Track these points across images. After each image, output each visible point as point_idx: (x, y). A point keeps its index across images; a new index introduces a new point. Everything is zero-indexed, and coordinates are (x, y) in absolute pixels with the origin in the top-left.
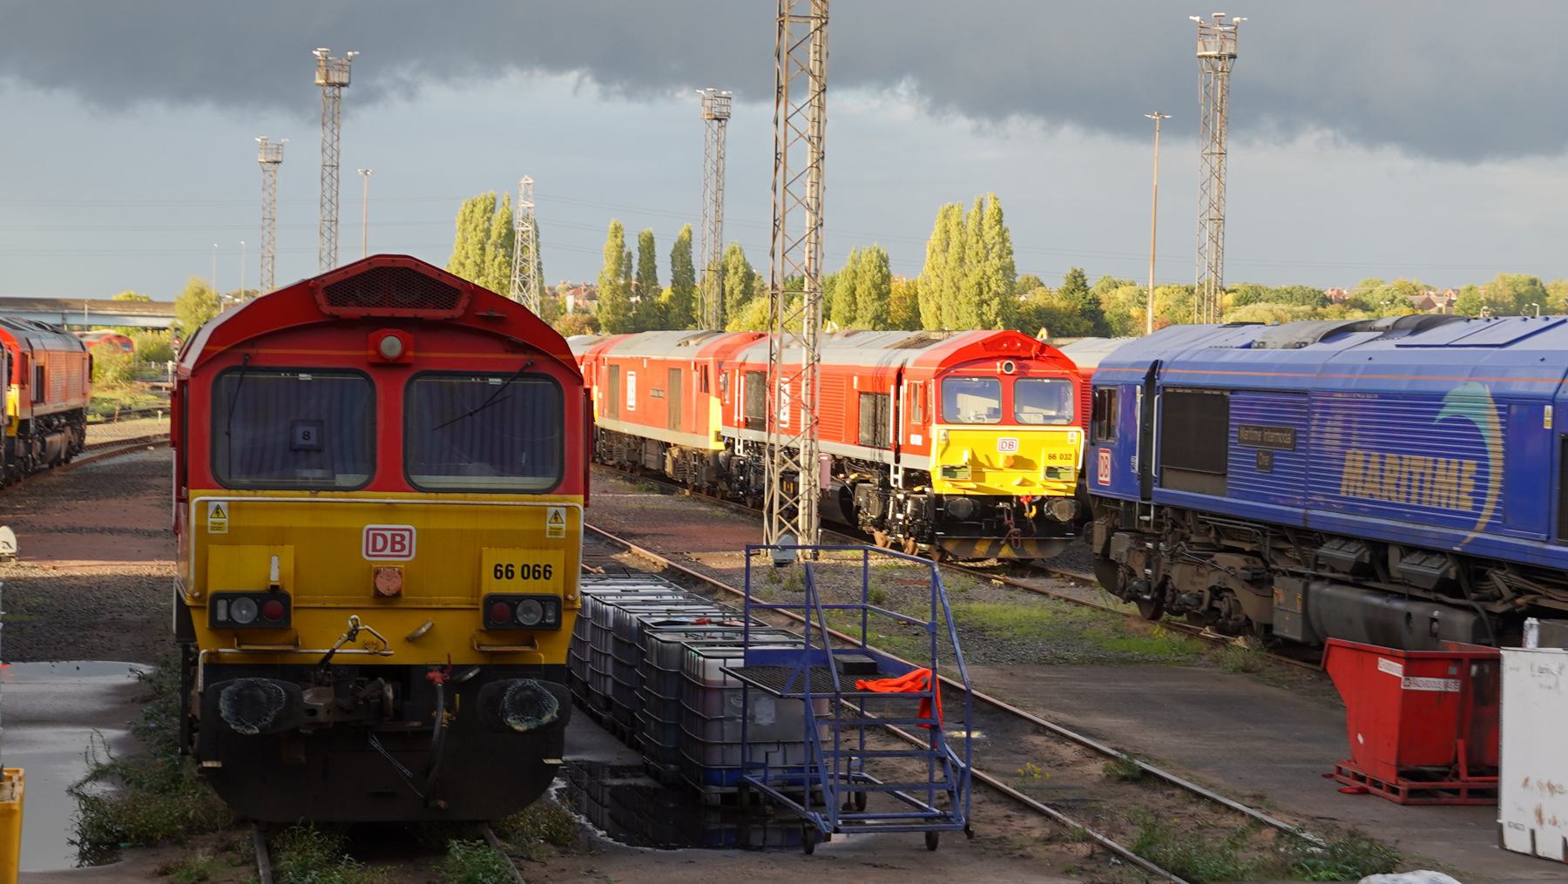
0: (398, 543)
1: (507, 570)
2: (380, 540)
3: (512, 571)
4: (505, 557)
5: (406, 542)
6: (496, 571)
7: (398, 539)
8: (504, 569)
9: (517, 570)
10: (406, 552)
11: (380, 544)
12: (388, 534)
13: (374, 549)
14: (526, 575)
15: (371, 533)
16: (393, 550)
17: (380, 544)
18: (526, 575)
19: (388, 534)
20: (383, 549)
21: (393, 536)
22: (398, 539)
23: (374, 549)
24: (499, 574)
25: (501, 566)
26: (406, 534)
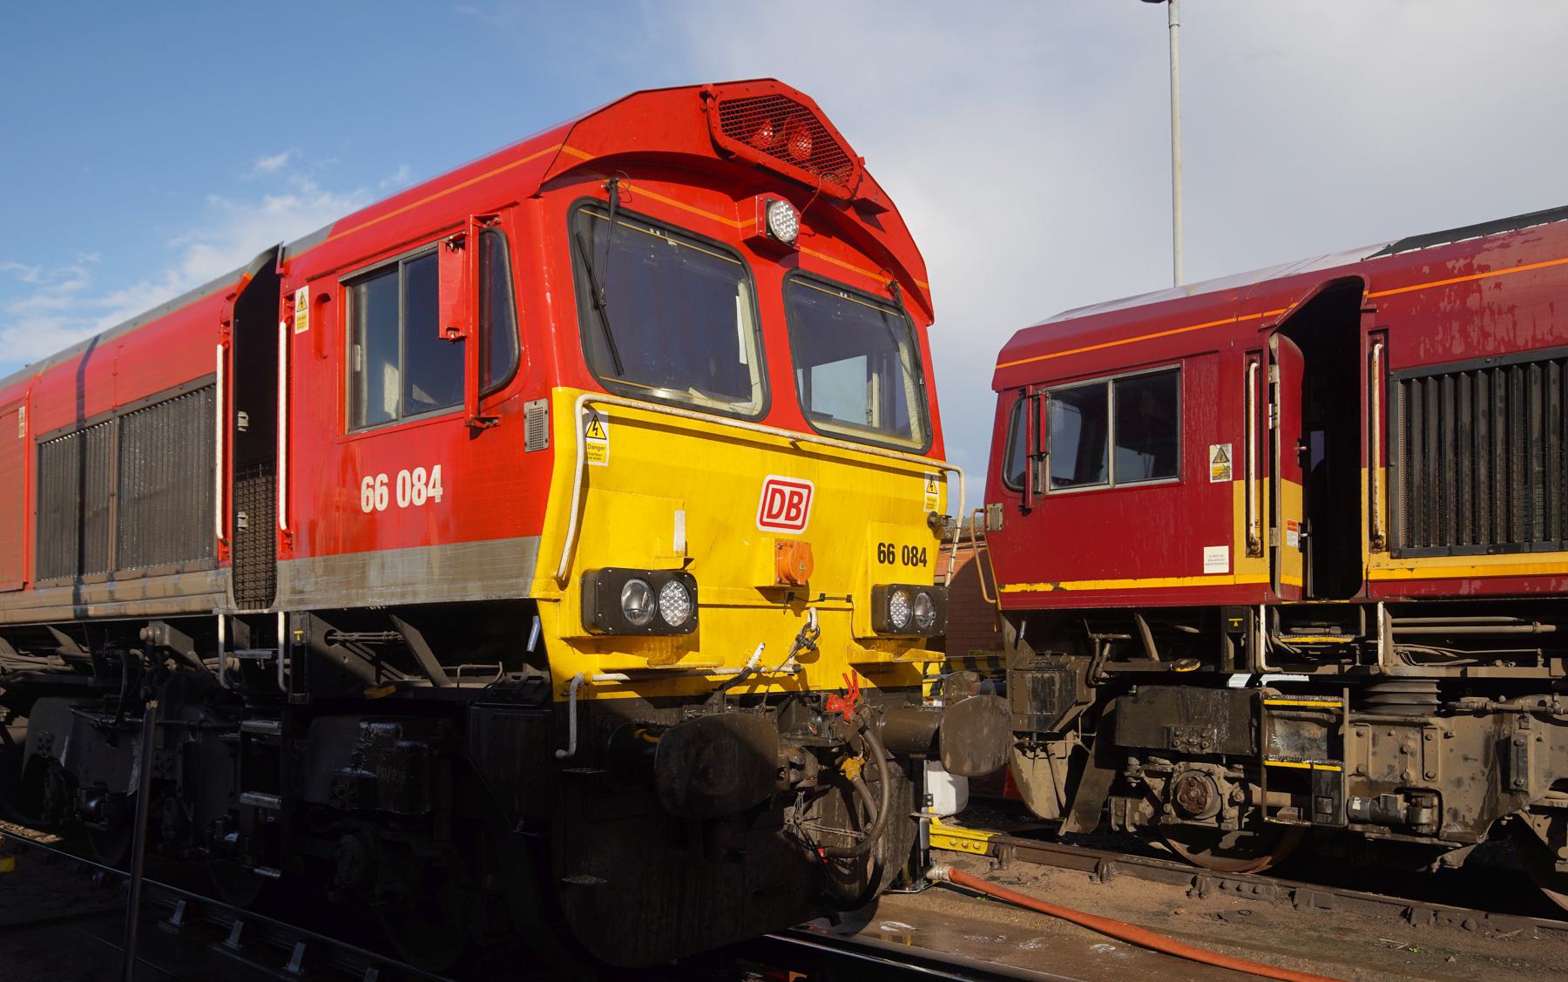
1: (889, 552)
2: (778, 496)
3: (893, 553)
5: (802, 506)
6: (880, 552)
7: (796, 499)
8: (886, 550)
10: (798, 522)
11: (775, 511)
12: (787, 490)
14: (906, 561)
16: (788, 517)
17: (775, 511)
18: (906, 561)
20: (777, 516)
21: (793, 494)
22: (796, 499)
26: (805, 492)
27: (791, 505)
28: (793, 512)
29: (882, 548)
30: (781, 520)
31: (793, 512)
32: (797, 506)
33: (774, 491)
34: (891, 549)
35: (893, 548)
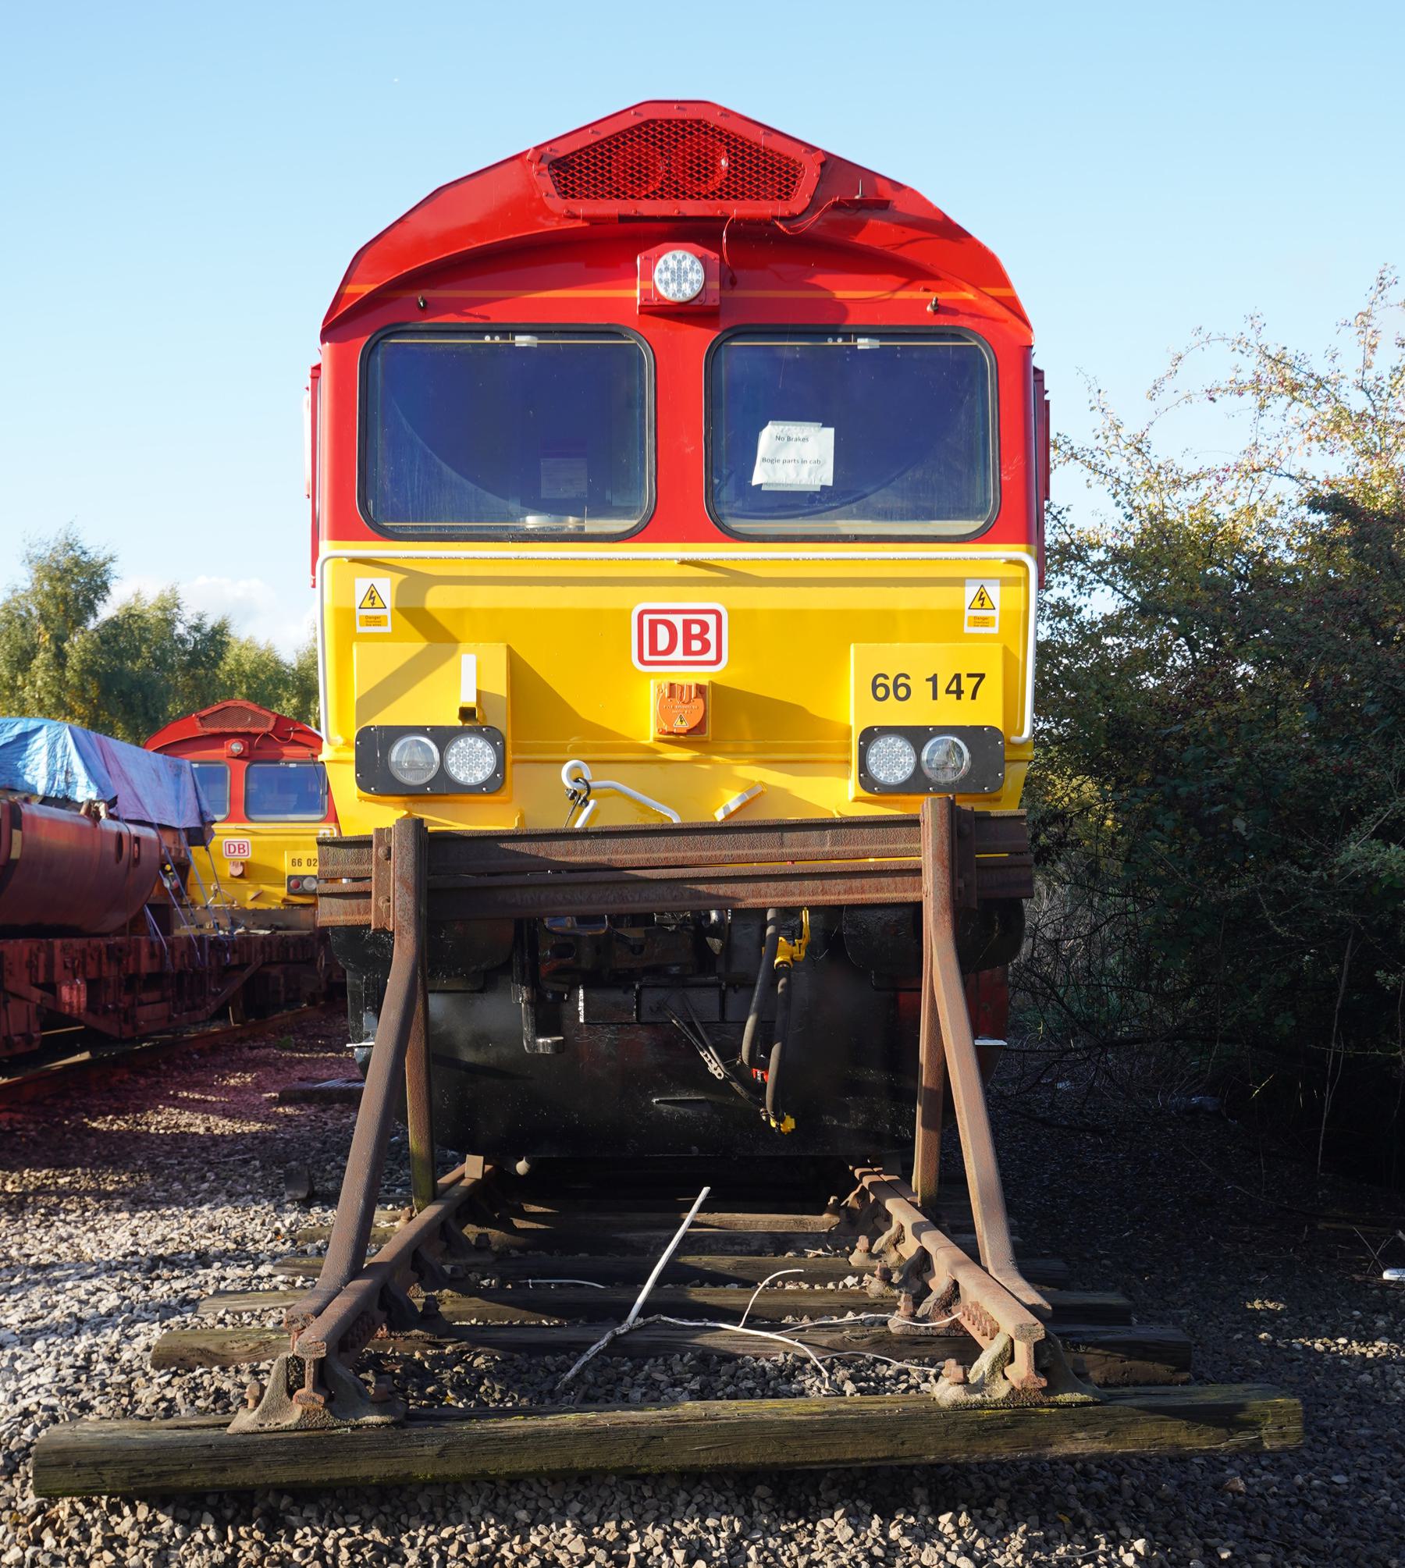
0: (700, 637)
1: (896, 687)
4: (892, 658)
5: (711, 636)
7: (696, 629)
8: (890, 683)
9: (921, 689)
10: (711, 655)
13: (653, 651)
15: (647, 618)
16: (687, 651)
19: (678, 621)
20: (671, 649)
21: (687, 624)
22: (696, 629)
23: (653, 651)
24: (881, 692)
25: (886, 677)
26: (711, 620)
27: (688, 637)
28: (696, 645)
29: (880, 680)
30: (678, 654)
31: (696, 645)
32: (700, 637)
33: (653, 624)
34: (901, 680)
35: (907, 677)
